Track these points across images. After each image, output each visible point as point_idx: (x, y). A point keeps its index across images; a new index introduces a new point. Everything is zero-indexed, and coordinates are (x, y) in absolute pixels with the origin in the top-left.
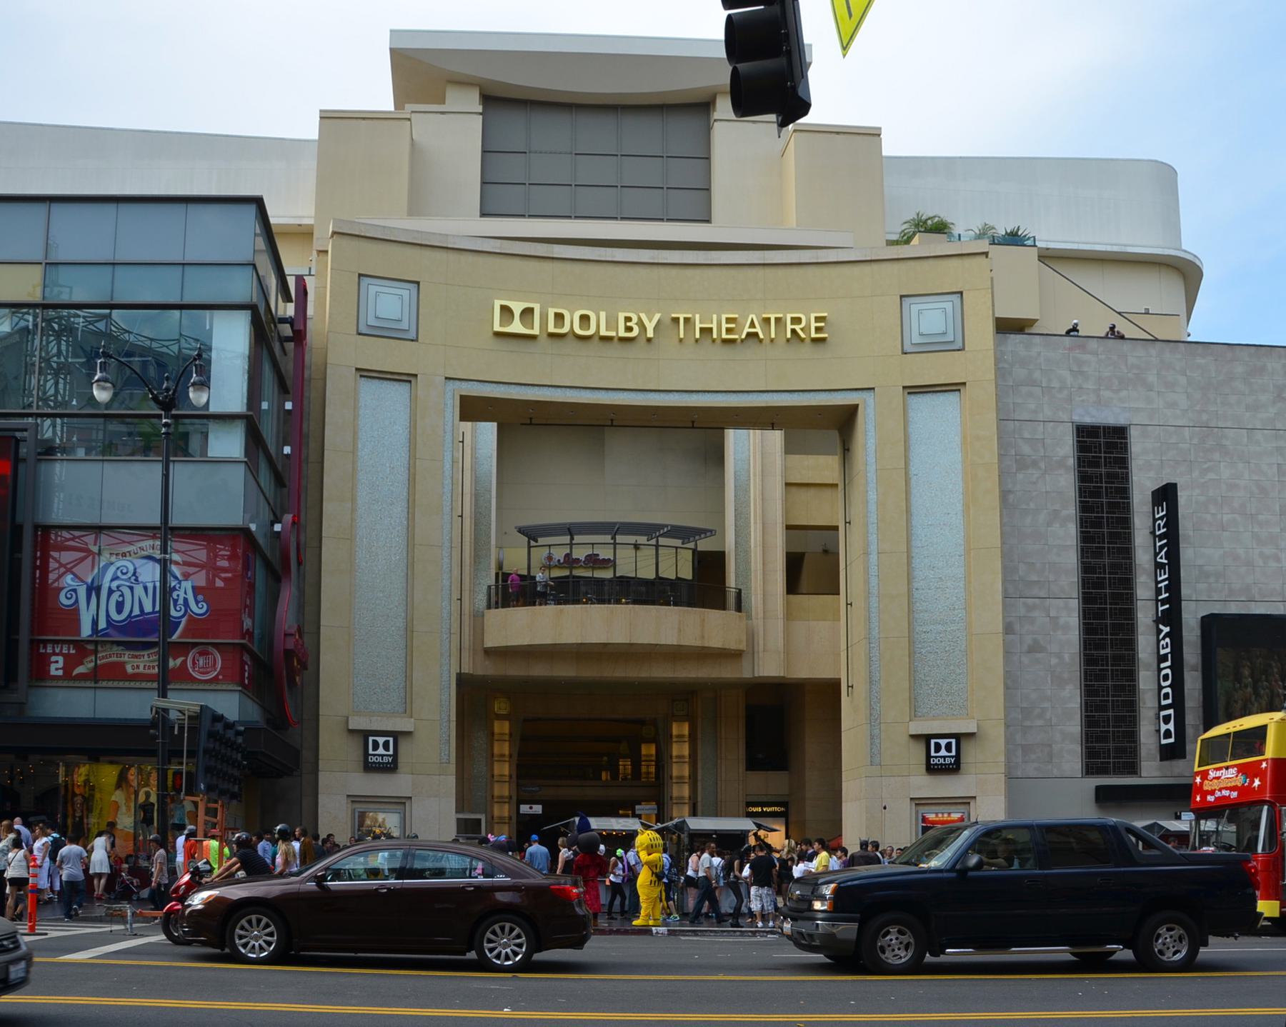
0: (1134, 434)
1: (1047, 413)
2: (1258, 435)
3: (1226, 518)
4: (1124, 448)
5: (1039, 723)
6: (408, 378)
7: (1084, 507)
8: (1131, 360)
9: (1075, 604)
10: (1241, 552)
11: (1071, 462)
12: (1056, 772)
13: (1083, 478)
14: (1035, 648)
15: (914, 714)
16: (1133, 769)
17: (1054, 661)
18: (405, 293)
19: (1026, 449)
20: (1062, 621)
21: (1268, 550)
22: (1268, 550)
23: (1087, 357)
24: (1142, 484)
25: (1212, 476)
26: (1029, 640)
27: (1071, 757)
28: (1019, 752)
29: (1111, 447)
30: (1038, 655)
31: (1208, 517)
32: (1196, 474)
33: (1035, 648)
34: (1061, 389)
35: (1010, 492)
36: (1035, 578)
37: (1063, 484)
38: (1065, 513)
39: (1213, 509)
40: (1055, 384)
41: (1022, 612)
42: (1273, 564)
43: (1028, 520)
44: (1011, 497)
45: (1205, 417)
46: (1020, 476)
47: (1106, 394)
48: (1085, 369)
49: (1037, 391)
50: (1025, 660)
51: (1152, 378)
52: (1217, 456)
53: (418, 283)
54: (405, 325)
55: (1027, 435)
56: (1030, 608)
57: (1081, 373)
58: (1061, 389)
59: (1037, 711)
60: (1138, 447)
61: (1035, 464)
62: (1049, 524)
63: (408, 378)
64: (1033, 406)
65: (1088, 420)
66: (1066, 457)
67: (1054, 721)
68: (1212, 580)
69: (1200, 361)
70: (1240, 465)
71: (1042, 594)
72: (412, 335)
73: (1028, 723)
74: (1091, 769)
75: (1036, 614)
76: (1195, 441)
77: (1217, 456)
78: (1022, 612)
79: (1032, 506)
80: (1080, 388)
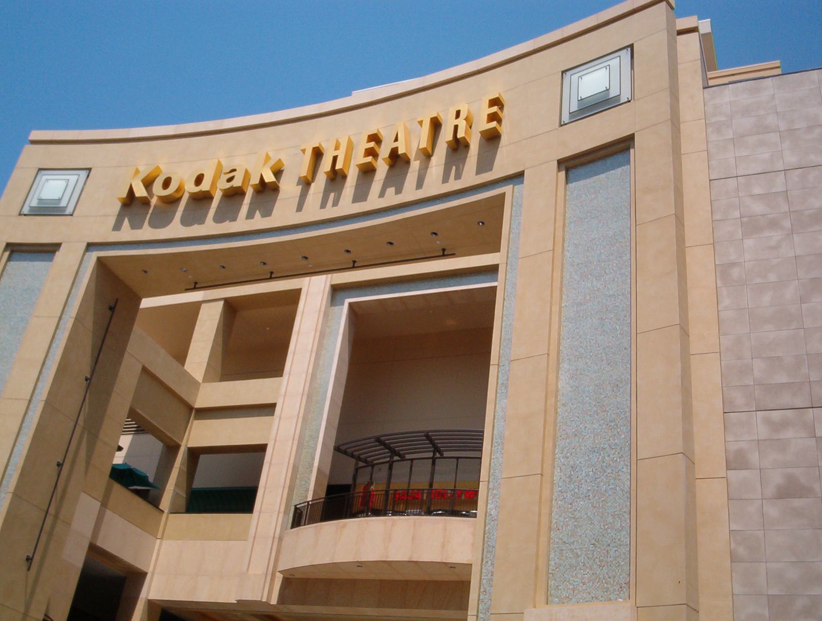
1: (791, 159)
19: (758, 208)
26: (777, 478)
30: (797, 503)
34: (810, 128)
35: (733, 264)
36: (782, 378)
43: (767, 298)
46: (749, 243)
49: (774, 137)
50: (773, 511)
55: (757, 190)
58: (810, 128)
59: (800, 603)
61: (774, 224)
75: (789, 434)
78: (763, 432)
79: (772, 277)
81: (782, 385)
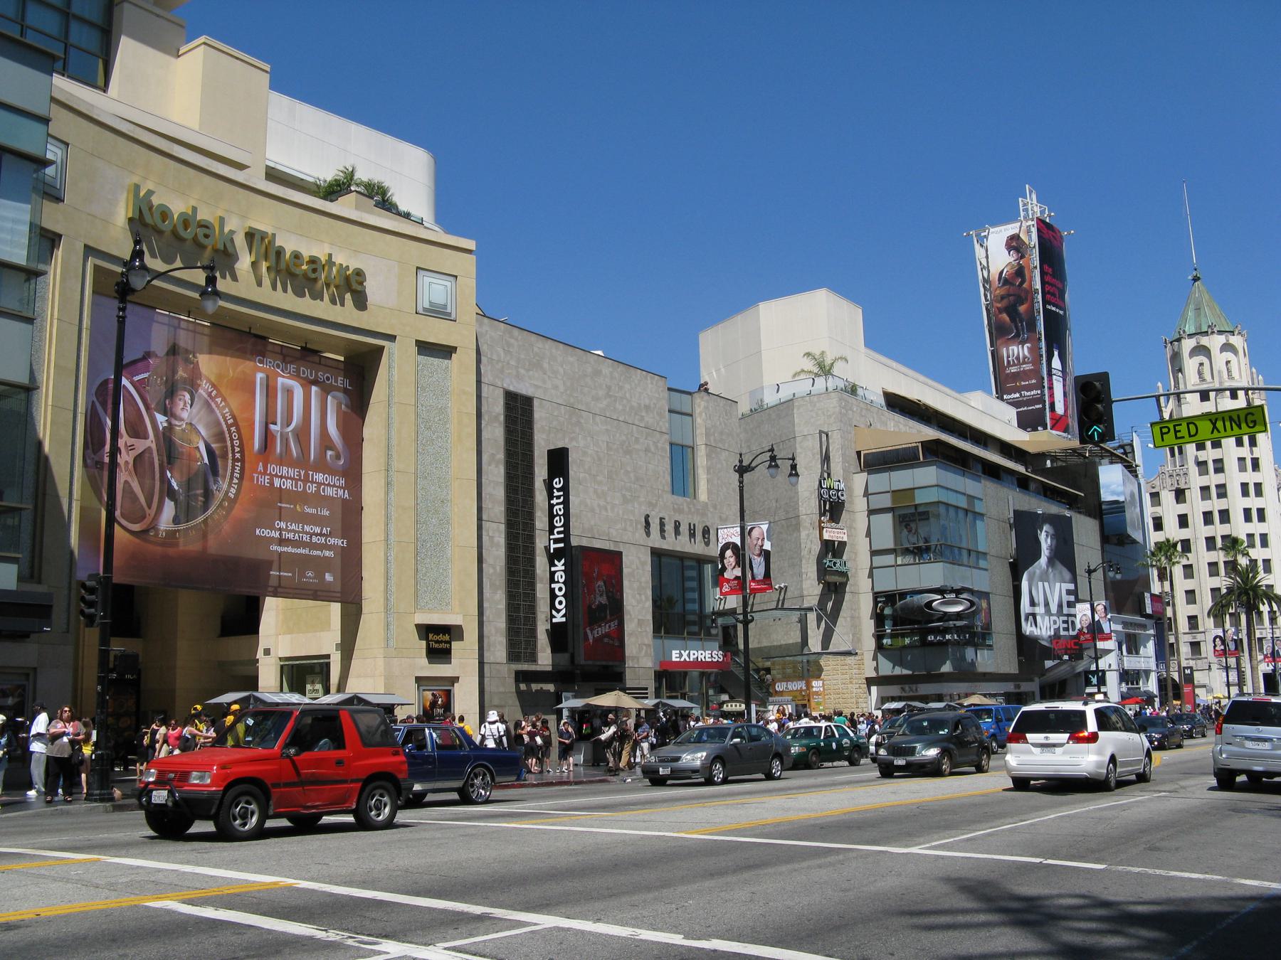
0: (536, 403)
2: (598, 418)
3: (582, 475)
9: (503, 527)
10: (588, 501)
11: (502, 418)
15: (417, 607)
16: (533, 658)
20: (496, 539)
23: (512, 341)
24: (542, 445)
34: (499, 361)
37: (495, 433)
40: (495, 357)
47: (522, 371)
51: (546, 365)
58: (499, 361)
60: (539, 414)
65: (511, 388)
69: (571, 359)
77: (577, 430)
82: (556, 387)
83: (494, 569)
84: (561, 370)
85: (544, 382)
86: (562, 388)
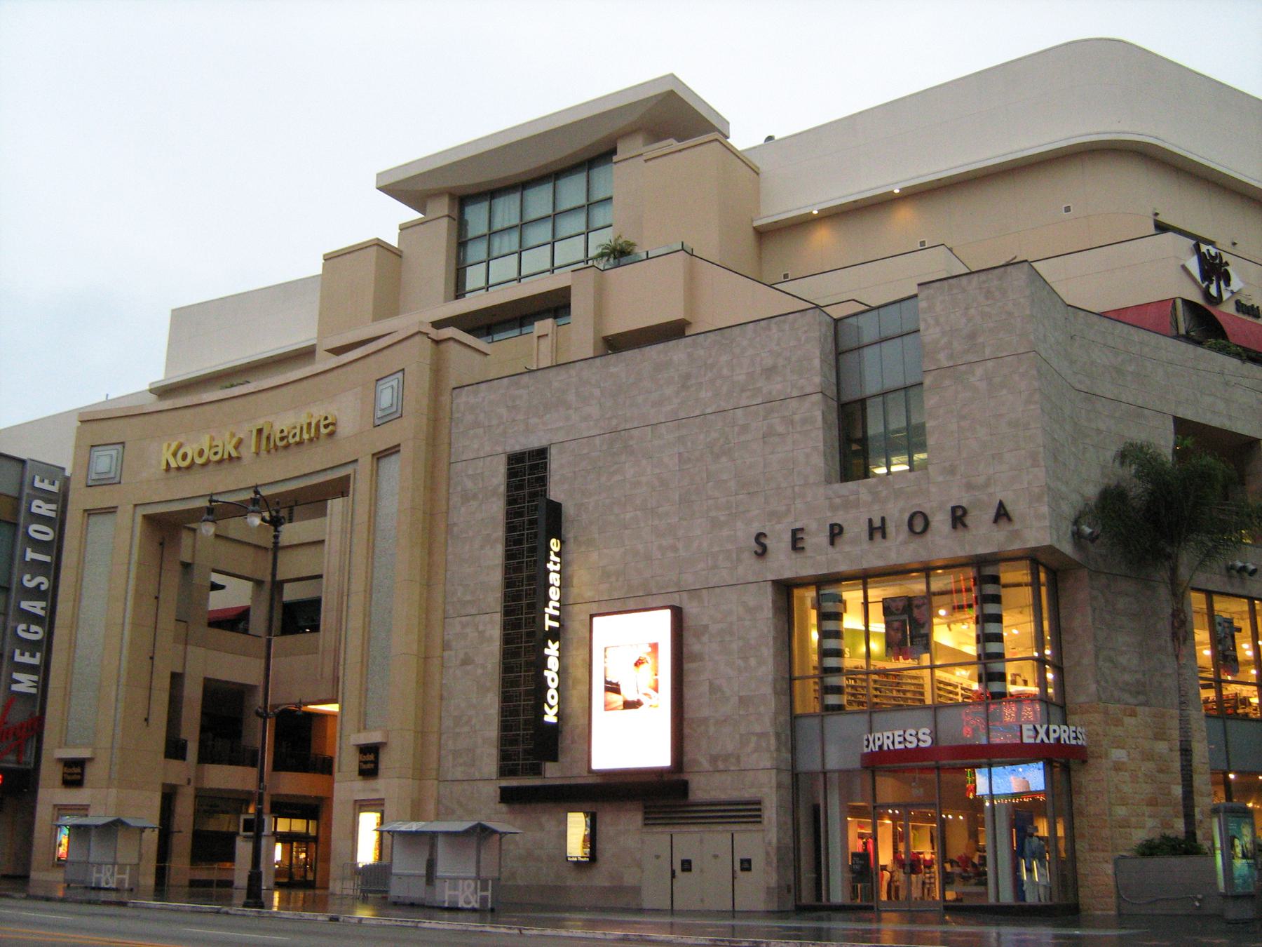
1: (487, 449)
3: (628, 516)
4: (544, 467)
5: (466, 729)
6: (112, 510)
7: (510, 528)
8: (556, 384)
9: (498, 618)
10: (640, 547)
11: (502, 489)
12: (477, 776)
13: (511, 501)
14: (466, 661)
17: (480, 671)
18: (114, 453)
19: (469, 484)
20: (487, 634)
21: (666, 542)
22: (664, 543)
25: (618, 477)
26: (461, 656)
27: (489, 762)
28: (450, 757)
29: (533, 468)
30: (469, 668)
31: (612, 518)
32: (603, 479)
33: (466, 661)
34: (499, 425)
35: (455, 524)
36: (468, 598)
38: (495, 535)
39: (616, 510)
40: (494, 422)
41: (458, 629)
42: (670, 554)
44: (455, 529)
45: (614, 422)
46: (463, 510)
47: (533, 421)
48: (518, 402)
49: (481, 430)
50: (458, 673)
51: (571, 397)
52: (623, 458)
53: (123, 443)
54: (112, 475)
55: (470, 472)
56: (464, 626)
57: (514, 407)
58: (499, 425)
60: (556, 464)
61: (475, 497)
62: (482, 547)
63: (112, 510)
64: (476, 446)
65: (517, 448)
66: (498, 486)
67: (478, 727)
68: (613, 579)
69: (613, 370)
70: (644, 462)
71: (473, 611)
72: (117, 480)
73: (457, 730)
74: (504, 772)
75: (468, 630)
76: (605, 447)
78: (458, 629)
80: (514, 421)
81: (469, 602)
82: (586, 418)
83: (483, 666)
84: (597, 392)
85: (568, 418)
86: (594, 410)
